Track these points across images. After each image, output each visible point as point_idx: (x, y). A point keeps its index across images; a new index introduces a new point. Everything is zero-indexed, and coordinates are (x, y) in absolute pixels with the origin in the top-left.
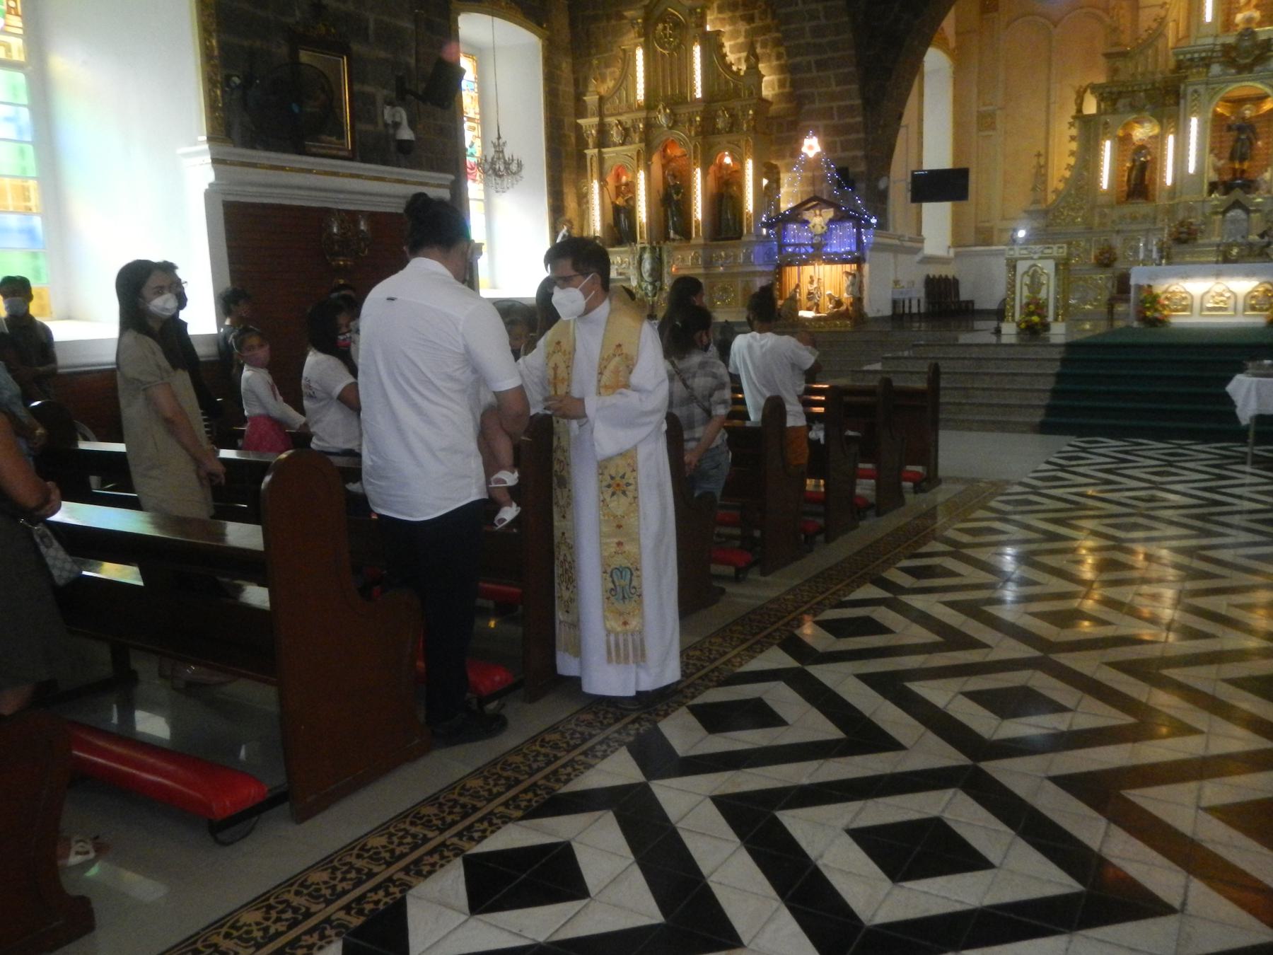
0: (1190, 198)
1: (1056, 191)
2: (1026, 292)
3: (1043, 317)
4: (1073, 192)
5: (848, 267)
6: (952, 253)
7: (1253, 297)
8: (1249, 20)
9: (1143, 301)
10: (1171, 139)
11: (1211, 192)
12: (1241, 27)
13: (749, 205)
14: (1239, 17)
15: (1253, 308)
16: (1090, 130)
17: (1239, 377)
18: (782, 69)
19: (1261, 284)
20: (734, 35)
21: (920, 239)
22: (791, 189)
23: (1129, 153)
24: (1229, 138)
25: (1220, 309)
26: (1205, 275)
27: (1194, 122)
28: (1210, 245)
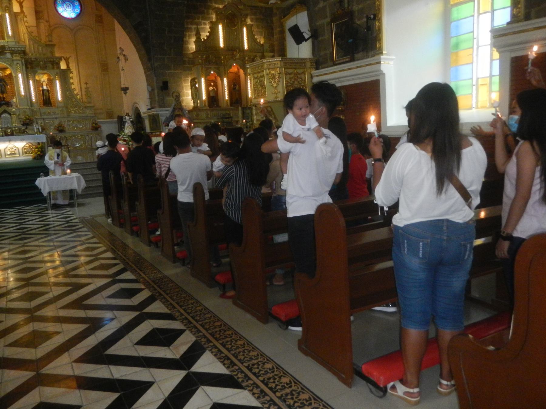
7: (25, 149)
15: (26, 153)
17: (38, 179)
19: (27, 143)
25: (13, 154)
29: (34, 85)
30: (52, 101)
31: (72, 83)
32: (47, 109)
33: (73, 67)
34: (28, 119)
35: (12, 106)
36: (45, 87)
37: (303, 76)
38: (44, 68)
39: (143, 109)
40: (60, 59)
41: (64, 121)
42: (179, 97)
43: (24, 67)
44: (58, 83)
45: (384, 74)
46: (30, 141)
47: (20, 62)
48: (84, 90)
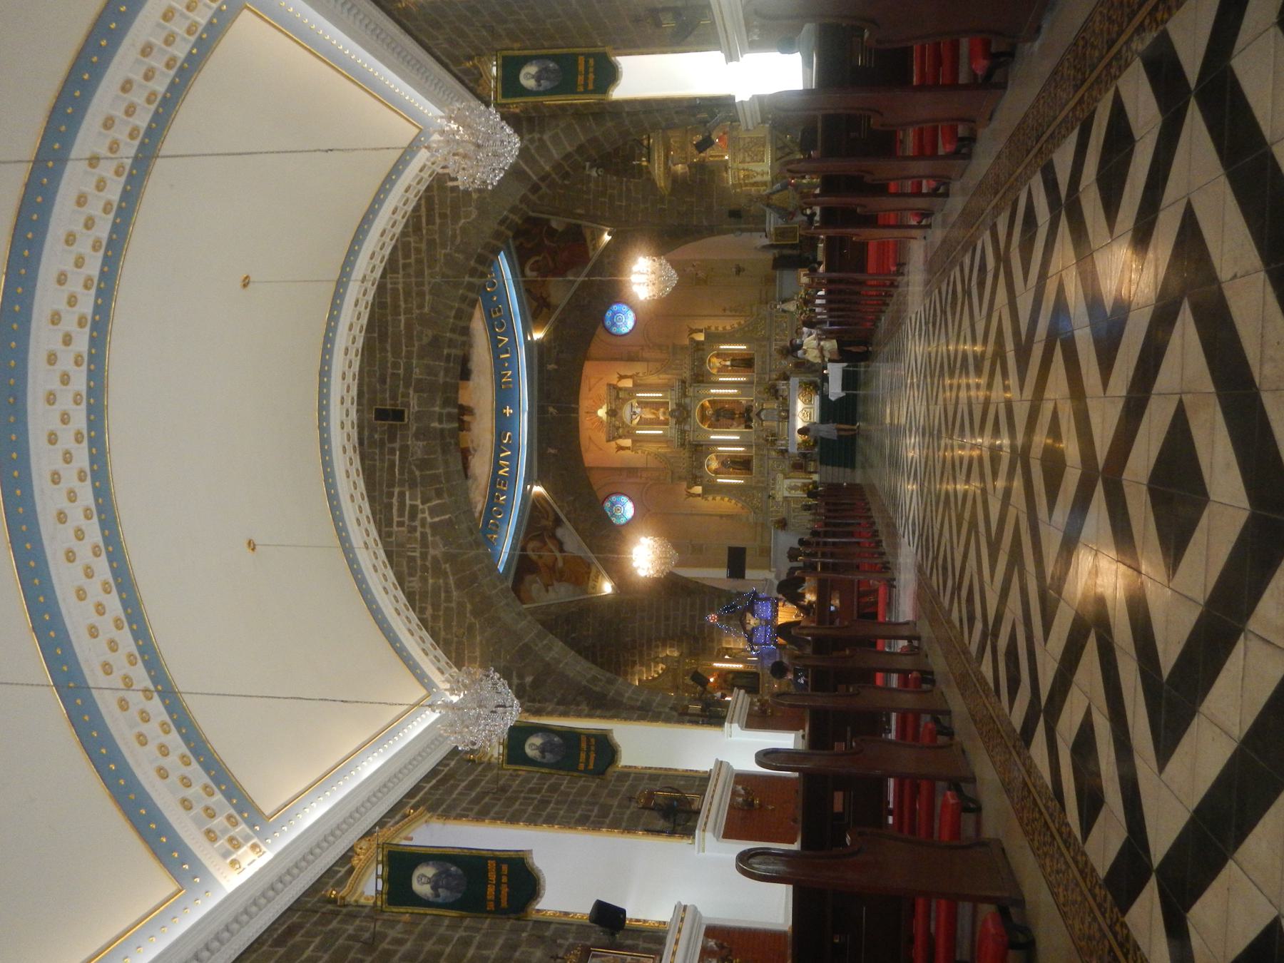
0: (753, 438)
1: (743, 508)
2: (799, 492)
3: (810, 484)
4: (743, 498)
5: (780, 608)
6: (772, 569)
8: (664, 413)
9: (806, 446)
10: (720, 449)
11: (751, 427)
12: (667, 416)
13: (739, 666)
14: (662, 418)
16: (712, 489)
18: (664, 645)
20: (641, 673)
21: (766, 580)
22: (732, 643)
23: (724, 470)
24: (723, 421)
26: (794, 420)
27: (712, 437)
28: (779, 426)
29: (724, 376)
30: (746, 357)
31: (724, 328)
32: (757, 363)
33: (704, 324)
34: (769, 390)
35: (752, 406)
36: (728, 363)
37: (749, 140)
38: (702, 361)
39: (767, 242)
40: (692, 340)
41: (776, 345)
42: (750, 195)
43: (702, 385)
44: (722, 347)
45: (753, 96)
46: (797, 394)
47: (696, 389)
48: (734, 313)
